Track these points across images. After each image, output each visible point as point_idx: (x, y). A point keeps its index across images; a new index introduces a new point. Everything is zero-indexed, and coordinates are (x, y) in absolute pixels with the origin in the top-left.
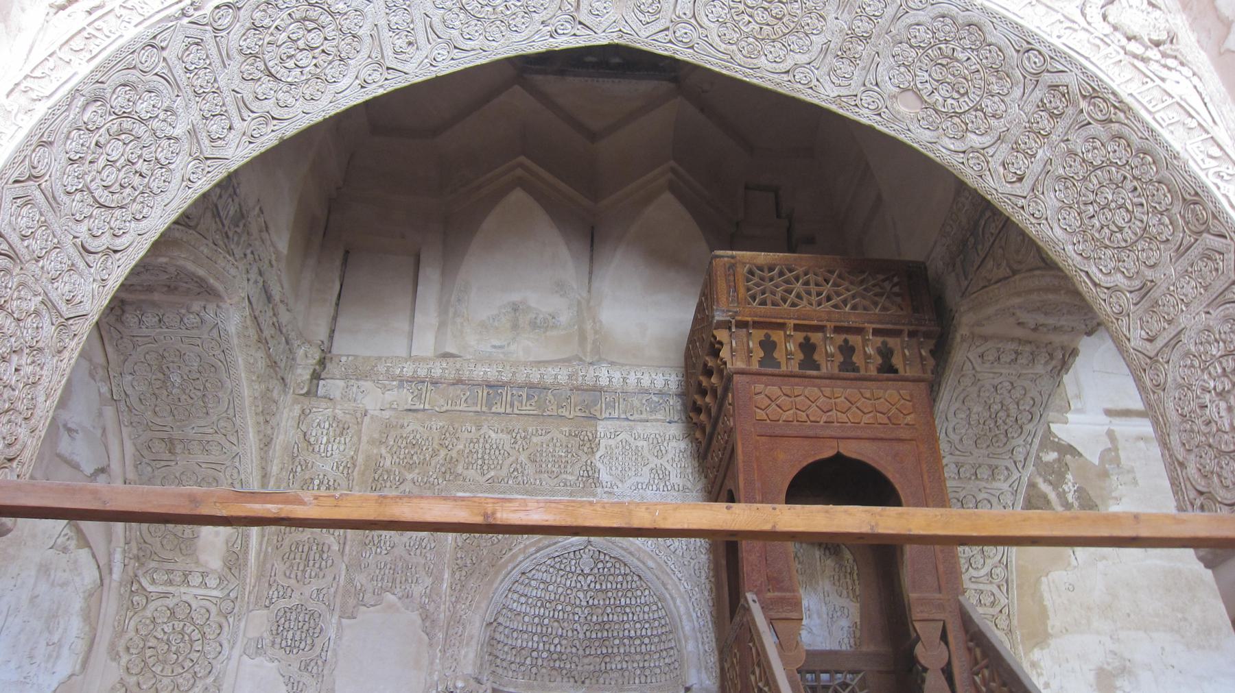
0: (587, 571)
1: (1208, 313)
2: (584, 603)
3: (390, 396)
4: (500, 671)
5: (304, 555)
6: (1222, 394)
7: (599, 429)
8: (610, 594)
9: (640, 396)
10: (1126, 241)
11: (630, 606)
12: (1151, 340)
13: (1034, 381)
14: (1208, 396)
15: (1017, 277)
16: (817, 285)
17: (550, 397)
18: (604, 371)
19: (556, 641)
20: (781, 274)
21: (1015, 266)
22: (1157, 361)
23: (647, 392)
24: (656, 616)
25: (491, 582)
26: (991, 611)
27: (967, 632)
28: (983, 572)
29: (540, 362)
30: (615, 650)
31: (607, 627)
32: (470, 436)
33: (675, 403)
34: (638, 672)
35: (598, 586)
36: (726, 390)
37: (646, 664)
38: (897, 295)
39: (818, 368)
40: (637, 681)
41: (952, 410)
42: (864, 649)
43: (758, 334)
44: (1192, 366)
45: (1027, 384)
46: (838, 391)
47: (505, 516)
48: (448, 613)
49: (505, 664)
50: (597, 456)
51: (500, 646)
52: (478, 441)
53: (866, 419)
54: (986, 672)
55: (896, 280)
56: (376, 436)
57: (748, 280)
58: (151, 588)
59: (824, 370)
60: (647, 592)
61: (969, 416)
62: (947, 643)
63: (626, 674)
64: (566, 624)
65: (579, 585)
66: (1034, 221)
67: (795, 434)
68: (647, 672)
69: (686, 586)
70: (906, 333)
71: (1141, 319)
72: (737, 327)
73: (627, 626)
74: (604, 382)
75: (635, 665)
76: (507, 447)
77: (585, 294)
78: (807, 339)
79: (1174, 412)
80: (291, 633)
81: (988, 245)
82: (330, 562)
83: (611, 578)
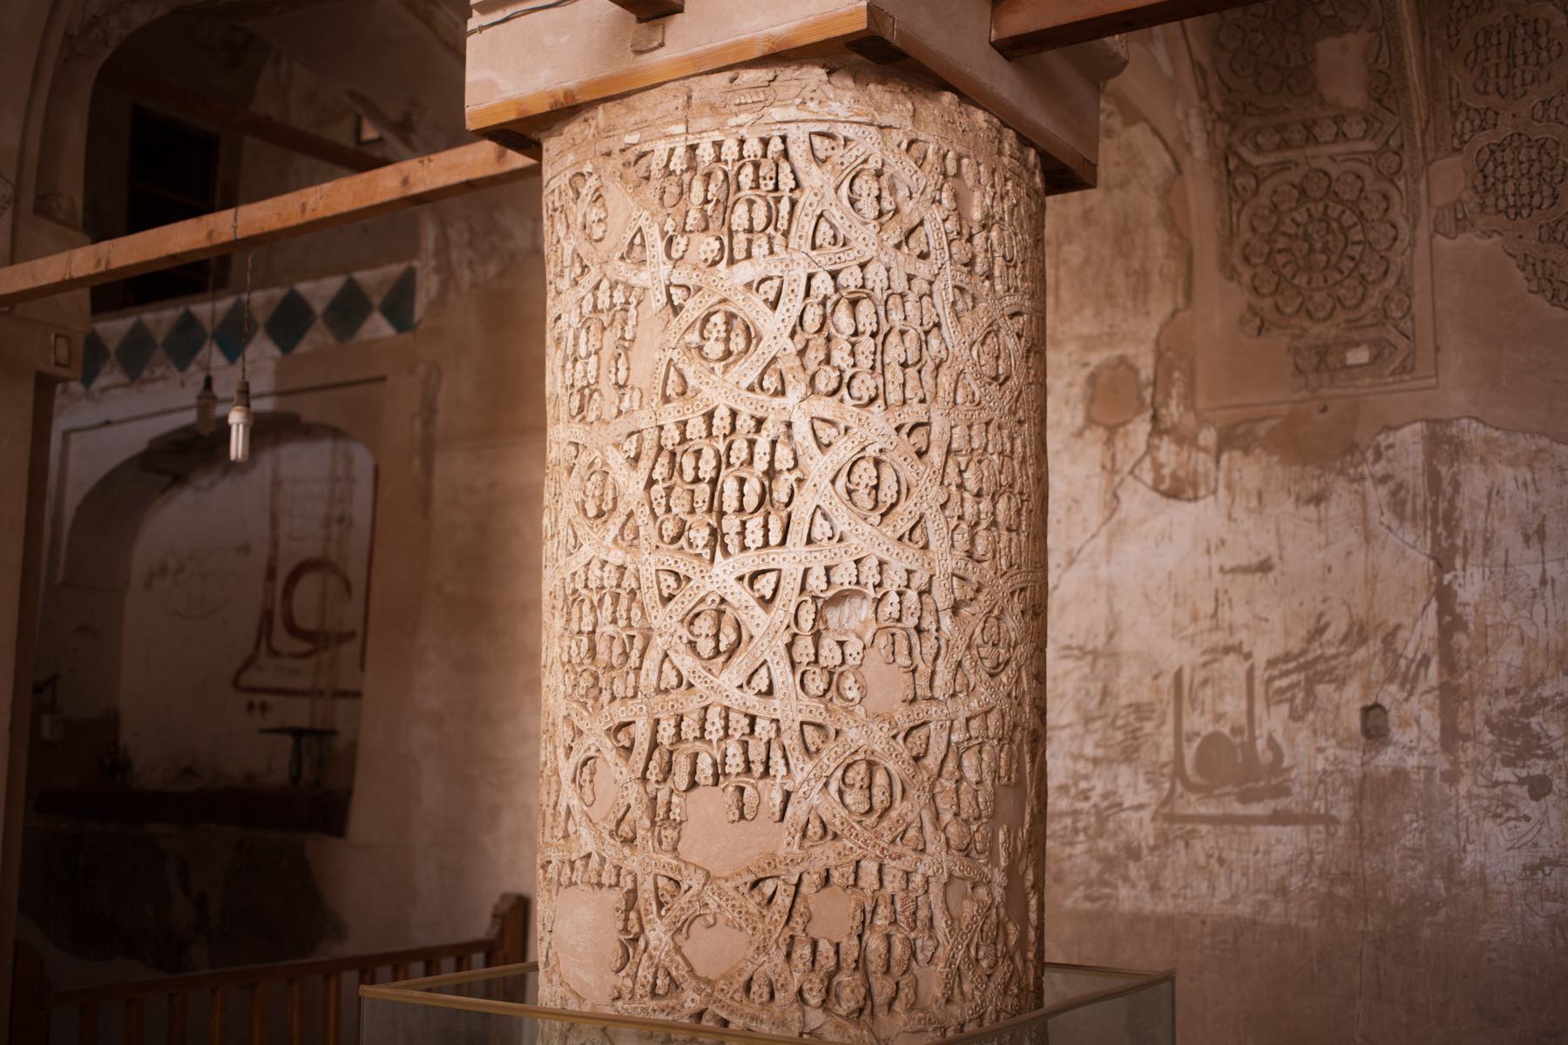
5: (1504, 50)
58: (1257, 161)
80: (1510, 183)
82: (1555, 49)
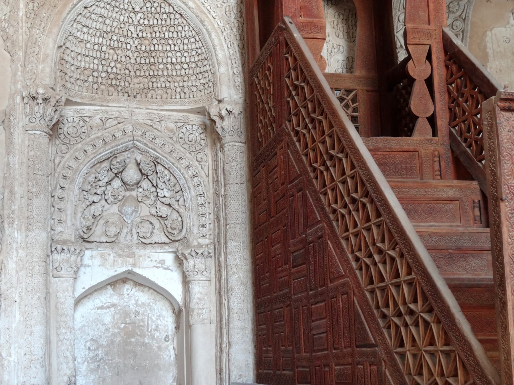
0: (137, 9)
2: (135, 35)
4: (69, 85)
8: (156, 29)
19: (112, 64)
24: (194, 47)
25: (60, 13)
30: (160, 73)
31: (153, 54)
37: (185, 84)
40: (178, 97)
48: (25, 36)
49: (72, 80)
51: (68, 65)
60: (187, 28)
64: (119, 52)
73: (170, 54)
75: (176, 84)
83: (157, 16)
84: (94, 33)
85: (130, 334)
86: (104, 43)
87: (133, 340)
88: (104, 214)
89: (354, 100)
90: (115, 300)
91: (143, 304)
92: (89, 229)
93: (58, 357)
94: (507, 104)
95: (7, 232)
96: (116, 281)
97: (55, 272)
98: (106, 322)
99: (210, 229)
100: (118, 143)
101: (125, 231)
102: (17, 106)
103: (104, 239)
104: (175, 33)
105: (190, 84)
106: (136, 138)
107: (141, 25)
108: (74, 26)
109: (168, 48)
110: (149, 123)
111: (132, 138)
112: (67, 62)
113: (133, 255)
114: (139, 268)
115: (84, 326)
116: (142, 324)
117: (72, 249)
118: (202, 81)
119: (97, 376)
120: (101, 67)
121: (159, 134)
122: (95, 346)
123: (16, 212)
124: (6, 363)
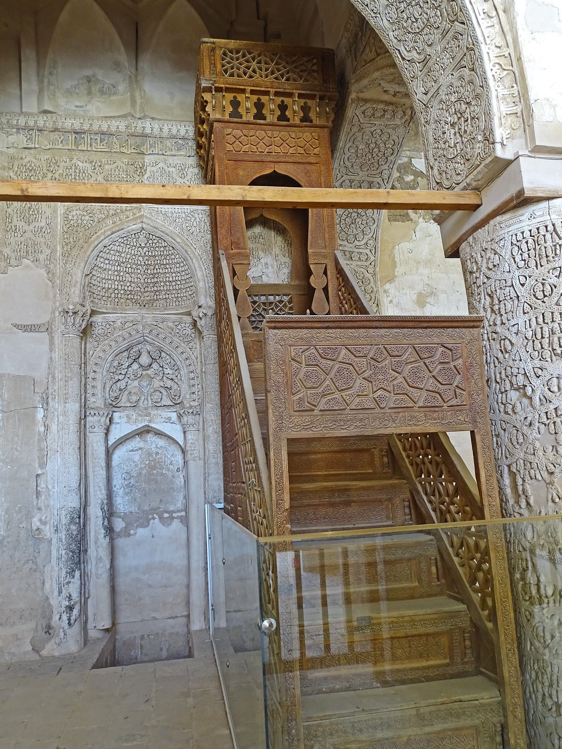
0: (143, 245)
1: (452, 75)
3: (11, 139)
4: (97, 301)
6: (453, 125)
7: (146, 161)
8: (157, 258)
9: (171, 140)
10: (419, 28)
11: (169, 264)
12: (426, 94)
13: (394, 129)
14: (447, 126)
15: (378, 58)
16: (266, 63)
17: (115, 140)
18: (148, 124)
19: (128, 284)
20: (244, 56)
21: (379, 51)
22: (428, 107)
23: (174, 137)
25: (85, 252)
26: (365, 264)
27: (337, 269)
28: (362, 243)
29: (107, 117)
30: (162, 288)
31: (157, 276)
32: (66, 164)
33: (192, 144)
34: (175, 299)
35: (150, 254)
36: (211, 132)
38: (314, 71)
39: (265, 119)
41: (347, 147)
42: (293, 283)
43: (230, 96)
44: (443, 109)
45: (390, 131)
46: (276, 133)
47: (34, 191)
49: (99, 297)
50: (145, 177)
51: (95, 287)
52: (71, 168)
53: (291, 151)
54: (343, 289)
55: (315, 61)
56: (6, 164)
57: (223, 59)
59: (268, 120)
60: (177, 256)
61: (357, 151)
62: (327, 276)
63: (168, 300)
64: (133, 275)
65: (139, 253)
66: (373, 15)
67: (250, 159)
68: (180, 299)
69: (198, 252)
70: (318, 97)
71: (423, 80)
72: (215, 91)
73: (168, 275)
74: (148, 131)
75: (173, 296)
76: (90, 172)
77: (133, 71)
78: (259, 99)
79: (432, 138)
81: (367, 37)
83: (157, 249)
84: (114, 264)
85: (153, 468)
86: (122, 270)
87: (155, 472)
88: (128, 387)
89: (290, 302)
90: (142, 445)
91: (161, 447)
92: (116, 398)
93: (94, 487)
94: (273, 325)
95: (51, 405)
96: (142, 432)
97: (91, 429)
98: (136, 460)
99: (198, 395)
100: (132, 338)
101: (143, 398)
102: (57, 318)
103: (128, 405)
104: (170, 260)
105: (182, 295)
106: (145, 335)
107: (147, 256)
108: (98, 259)
109: (167, 271)
110: (155, 323)
111: (142, 335)
112: (94, 285)
113: (149, 415)
114: (154, 423)
115: (120, 463)
116: (161, 460)
117: (101, 413)
118: (190, 293)
119: (130, 497)
120: (120, 286)
121: (162, 331)
122: (129, 477)
123: (57, 391)
124: (51, 493)
